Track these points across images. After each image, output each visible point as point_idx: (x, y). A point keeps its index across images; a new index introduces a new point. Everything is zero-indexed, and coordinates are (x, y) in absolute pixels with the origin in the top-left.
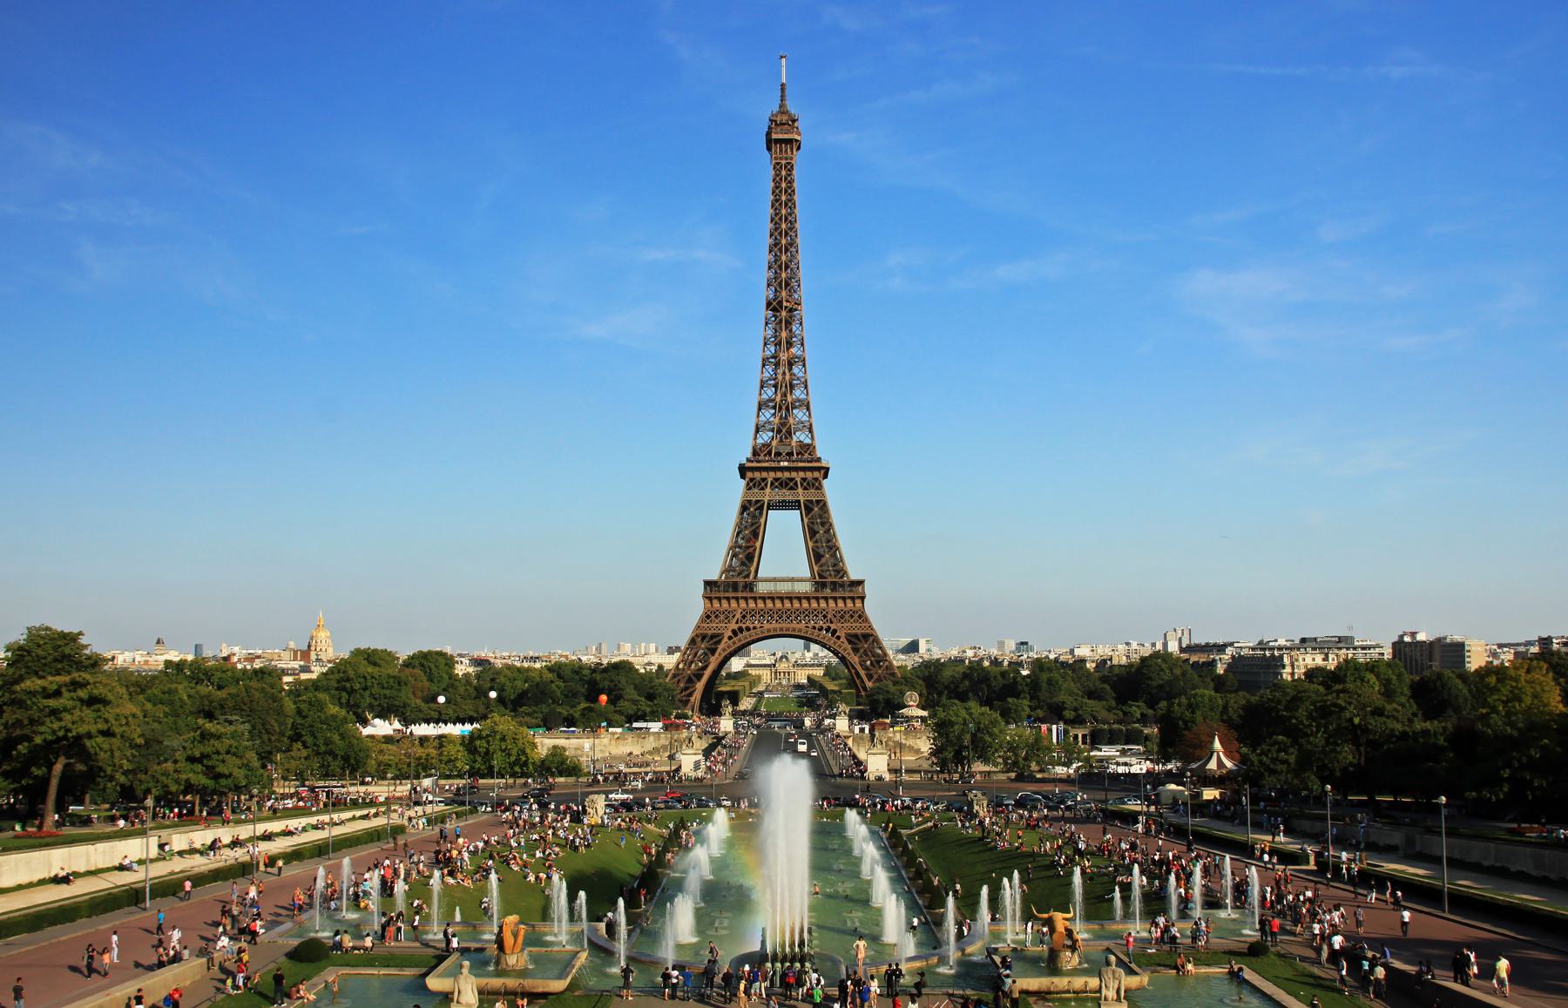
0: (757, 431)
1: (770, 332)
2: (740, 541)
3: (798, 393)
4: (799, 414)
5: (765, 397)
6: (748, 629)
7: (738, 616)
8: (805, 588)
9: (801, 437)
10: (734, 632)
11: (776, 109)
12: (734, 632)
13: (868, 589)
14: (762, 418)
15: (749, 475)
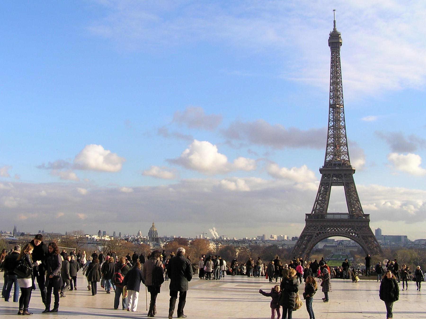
0: (326, 155)
1: (331, 117)
2: (320, 198)
3: (343, 140)
4: (343, 149)
5: (329, 142)
6: (323, 233)
7: (319, 228)
8: (346, 217)
9: (344, 157)
10: (317, 234)
11: (332, 30)
12: (317, 234)
13: (371, 218)
14: (329, 150)
15: (324, 173)
